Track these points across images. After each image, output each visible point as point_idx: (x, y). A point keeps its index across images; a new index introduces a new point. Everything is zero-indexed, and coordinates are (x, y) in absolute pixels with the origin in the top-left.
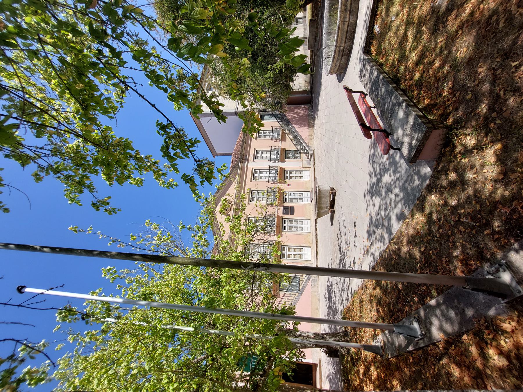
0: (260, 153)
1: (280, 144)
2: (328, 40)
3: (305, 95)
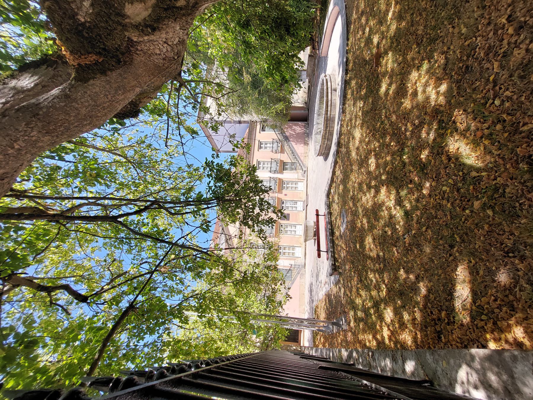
0: (262, 164)
1: (279, 156)
2: (318, 119)
3: (303, 111)
